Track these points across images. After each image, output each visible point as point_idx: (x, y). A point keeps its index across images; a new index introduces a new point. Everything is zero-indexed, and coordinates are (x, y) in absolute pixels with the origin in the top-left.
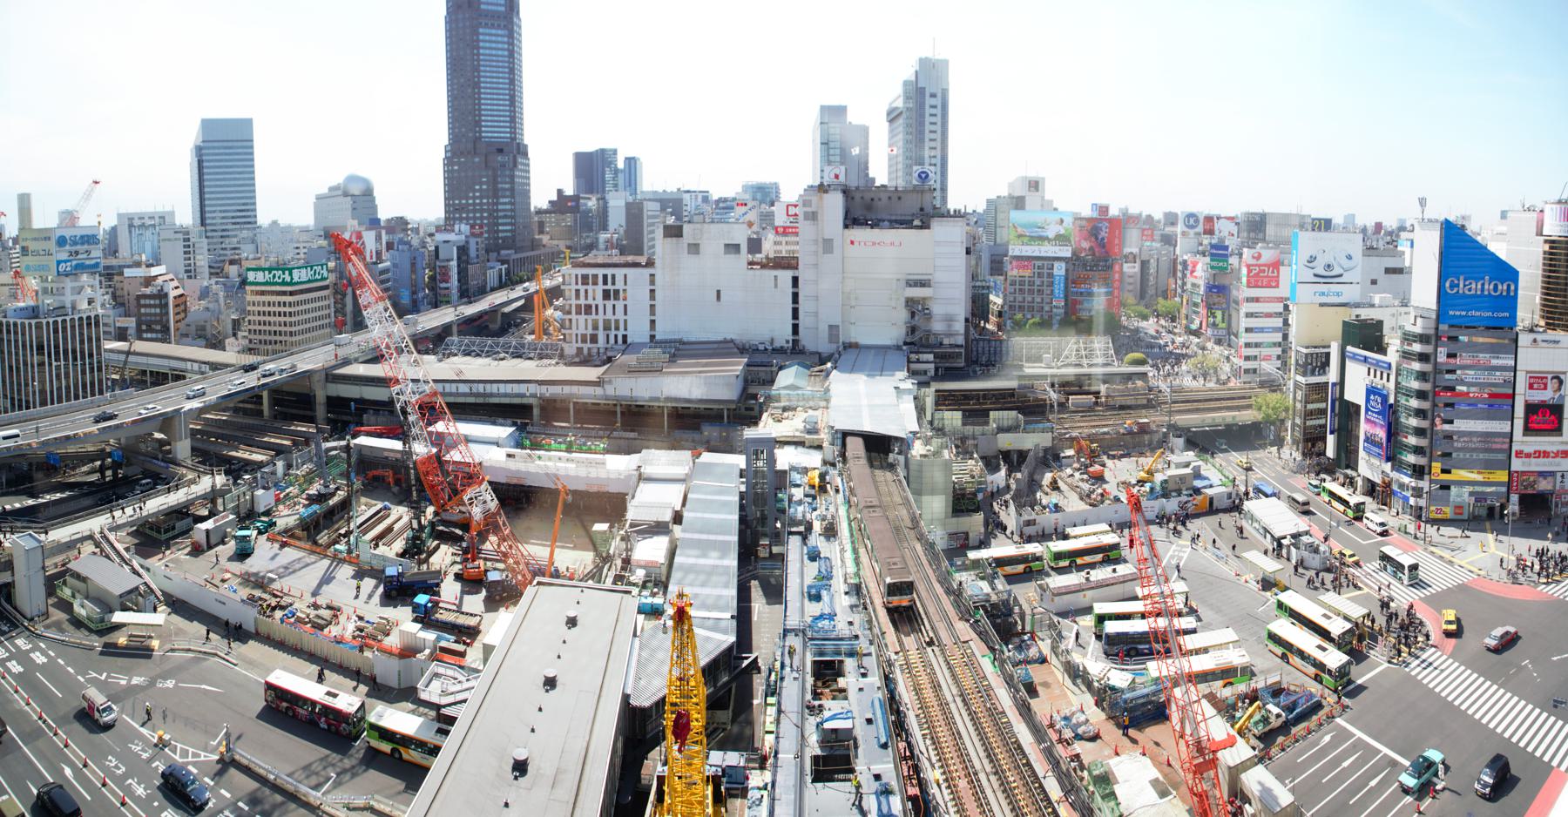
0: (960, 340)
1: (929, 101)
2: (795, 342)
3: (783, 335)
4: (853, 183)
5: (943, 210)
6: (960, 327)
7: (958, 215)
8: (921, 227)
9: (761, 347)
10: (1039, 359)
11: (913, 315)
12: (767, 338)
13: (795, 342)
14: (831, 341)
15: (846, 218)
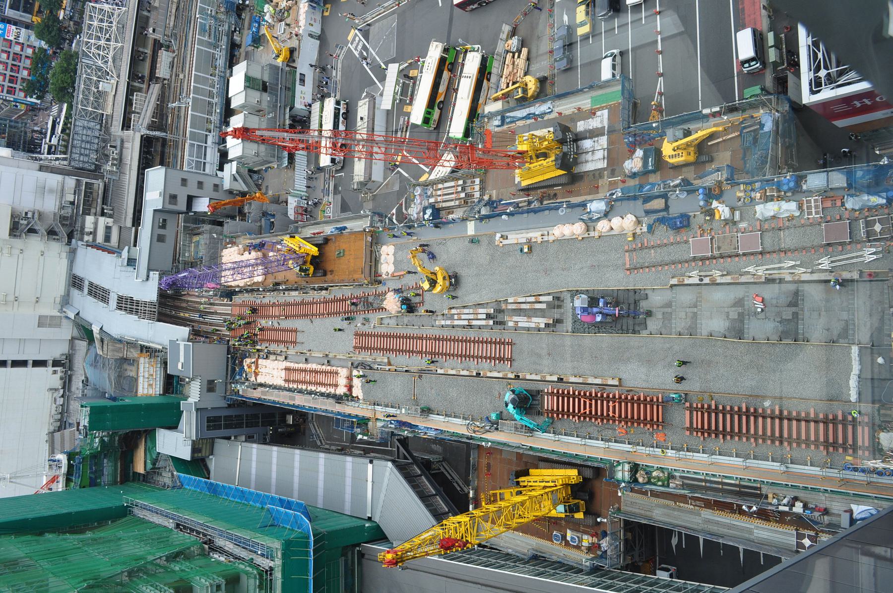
0: (71, 182)
2: (56, 363)
3: (50, 377)
6: (54, 180)
9: (60, 401)
10: (100, 95)
11: (32, 231)
12: (49, 395)
13: (56, 363)
14: (59, 326)
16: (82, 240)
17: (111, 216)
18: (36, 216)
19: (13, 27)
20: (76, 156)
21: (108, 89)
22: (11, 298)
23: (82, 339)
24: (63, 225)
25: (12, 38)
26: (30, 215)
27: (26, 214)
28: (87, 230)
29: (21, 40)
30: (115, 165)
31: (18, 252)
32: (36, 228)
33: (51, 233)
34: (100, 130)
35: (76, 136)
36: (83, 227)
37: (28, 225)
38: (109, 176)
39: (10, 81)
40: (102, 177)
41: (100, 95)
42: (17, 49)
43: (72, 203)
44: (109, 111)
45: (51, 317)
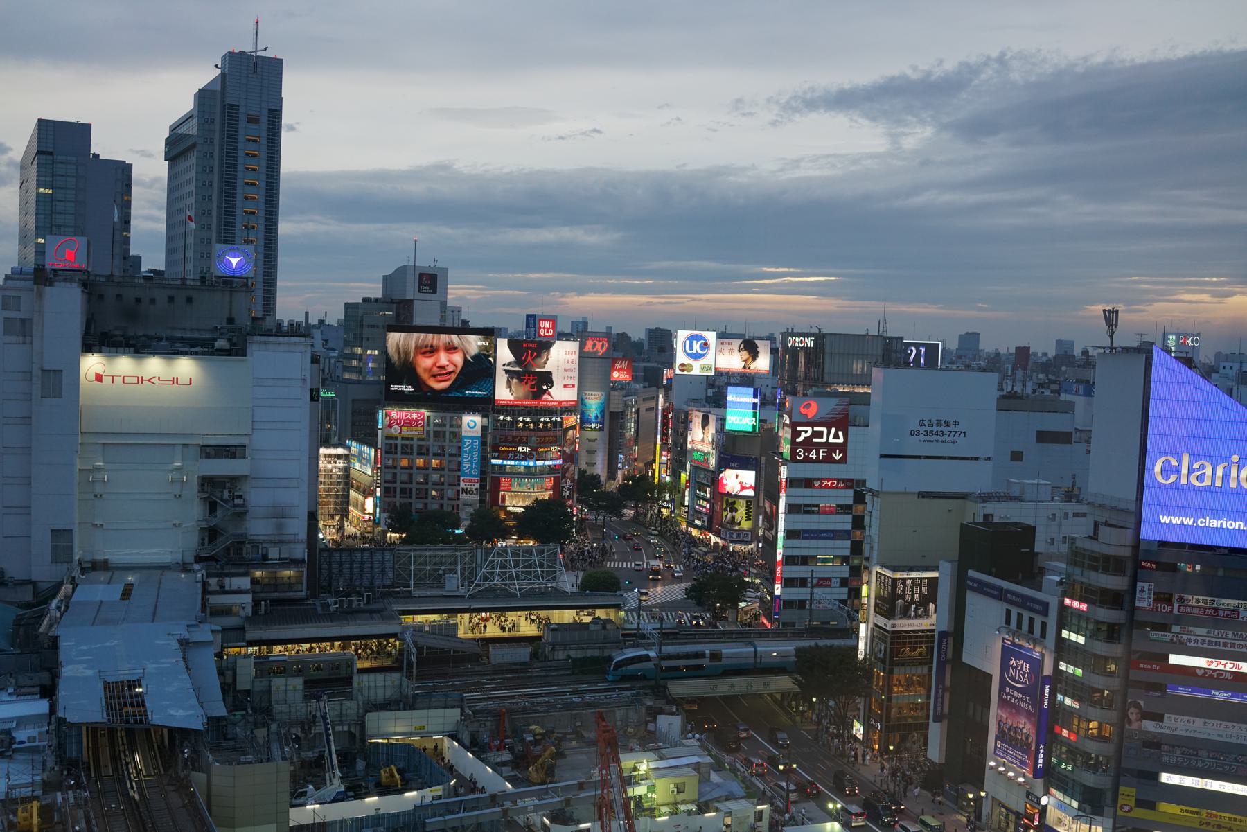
0: (300, 551)
1: (245, 130)
4: (102, 269)
5: (268, 323)
6: (298, 528)
7: (296, 330)
8: (229, 353)
11: (212, 507)
14: (55, 560)
15: (87, 333)
16: (209, 575)
17: (255, 612)
18: (238, 510)
19: (477, 485)
20: (337, 556)
21: (448, 586)
22: (99, 489)
23: (35, 594)
24: (227, 549)
25: (462, 485)
26: (237, 501)
27: (240, 497)
28: (227, 580)
29: (463, 496)
30: (341, 606)
31: (178, 493)
32: (219, 512)
33: (211, 534)
34: (384, 586)
35: (367, 554)
36: (228, 575)
37: (222, 500)
38: (318, 604)
39: (403, 491)
40: (313, 595)
41: (438, 580)
42: (450, 493)
43: (265, 557)
44: (417, 593)
45: (71, 548)
